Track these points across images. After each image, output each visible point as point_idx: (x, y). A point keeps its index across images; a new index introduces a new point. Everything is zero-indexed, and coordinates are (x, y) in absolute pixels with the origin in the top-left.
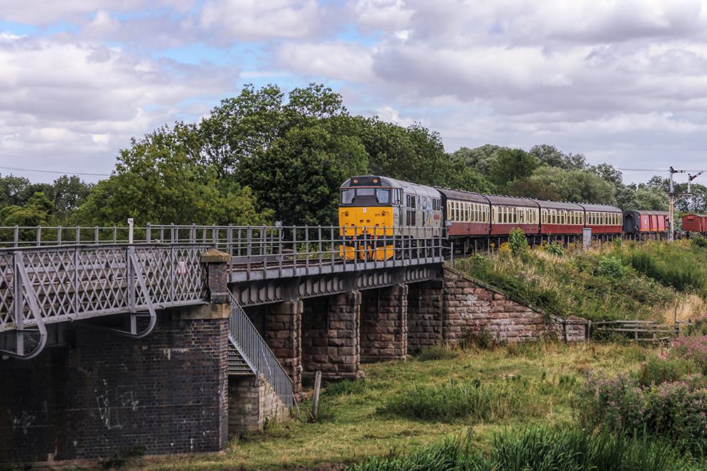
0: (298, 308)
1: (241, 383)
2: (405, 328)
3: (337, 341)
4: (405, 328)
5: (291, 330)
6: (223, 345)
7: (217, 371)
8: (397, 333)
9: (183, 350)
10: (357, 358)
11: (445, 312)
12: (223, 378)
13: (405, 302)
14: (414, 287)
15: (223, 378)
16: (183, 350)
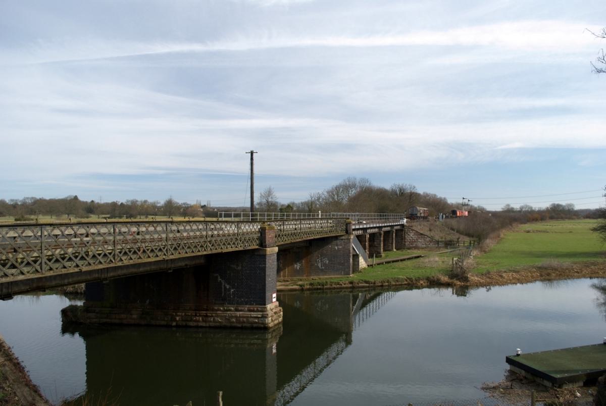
0: (368, 236)
1: (356, 256)
2: (394, 242)
3: (377, 245)
4: (394, 242)
5: (366, 242)
6: (351, 247)
7: (350, 253)
8: (392, 243)
9: (341, 247)
10: (382, 250)
11: (405, 238)
12: (351, 255)
13: (394, 235)
14: (396, 230)
15: (351, 255)
16: (341, 247)
